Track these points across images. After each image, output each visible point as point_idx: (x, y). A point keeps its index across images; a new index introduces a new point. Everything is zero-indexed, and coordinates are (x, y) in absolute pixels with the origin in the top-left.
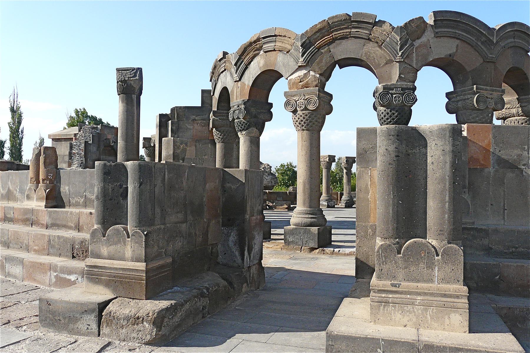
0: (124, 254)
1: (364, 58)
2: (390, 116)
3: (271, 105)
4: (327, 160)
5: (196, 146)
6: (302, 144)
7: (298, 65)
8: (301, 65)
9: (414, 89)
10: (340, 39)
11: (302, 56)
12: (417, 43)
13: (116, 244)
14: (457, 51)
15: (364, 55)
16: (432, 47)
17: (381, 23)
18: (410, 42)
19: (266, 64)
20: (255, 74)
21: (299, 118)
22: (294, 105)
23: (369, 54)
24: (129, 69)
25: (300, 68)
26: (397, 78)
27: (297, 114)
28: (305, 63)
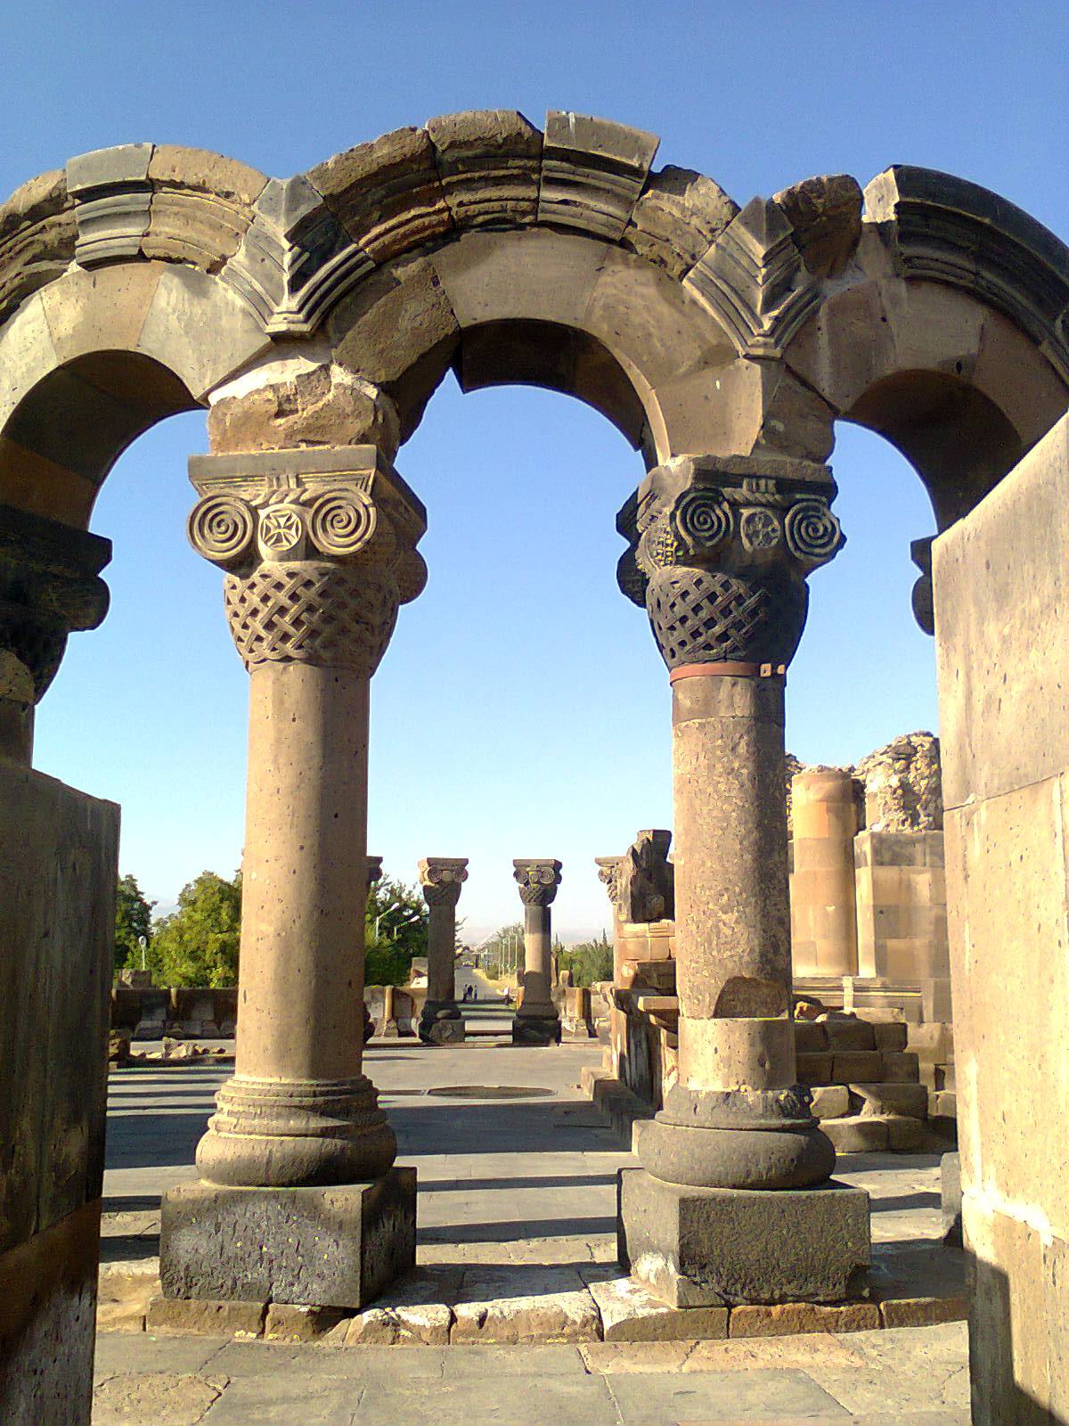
2: (726, 612)
3: (102, 550)
6: (279, 731)
7: (271, 329)
9: (830, 490)
10: (486, 227)
11: (295, 286)
12: (833, 290)
15: (598, 312)
16: (890, 316)
19: (90, 323)
20: (30, 370)
21: (265, 599)
22: (241, 526)
23: (627, 313)
25: (282, 345)
27: (255, 577)
28: (306, 321)
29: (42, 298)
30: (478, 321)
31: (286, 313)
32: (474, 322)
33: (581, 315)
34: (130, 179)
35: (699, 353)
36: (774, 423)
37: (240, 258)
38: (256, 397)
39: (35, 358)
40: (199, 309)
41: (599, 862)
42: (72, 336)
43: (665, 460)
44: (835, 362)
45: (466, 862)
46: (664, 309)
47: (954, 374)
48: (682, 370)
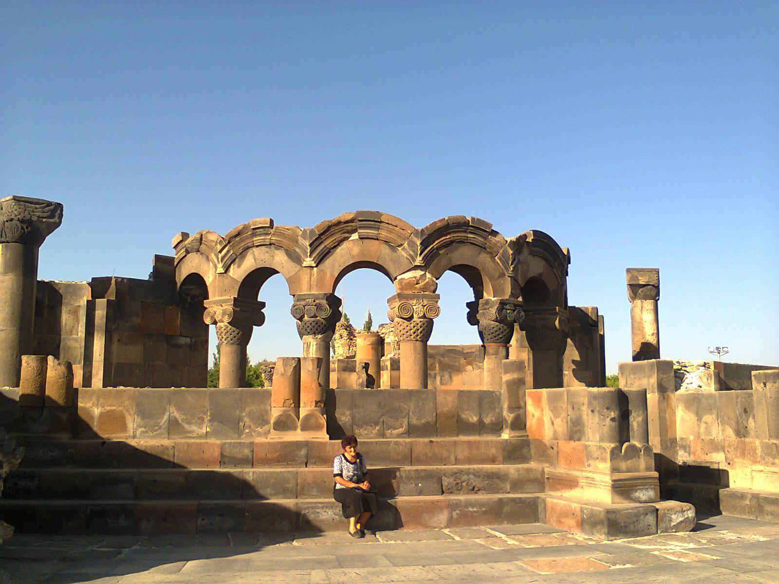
0: (639, 466)
2: (502, 333)
5: (144, 345)
6: (415, 357)
8: (419, 264)
10: (458, 242)
11: (421, 254)
13: (631, 458)
17: (495, 233)
19: (362, 252)
20: (344, 263)
21: (414, 327)
24: (41, 202)
25: (416, 268)
27: (412, 321)
28: (423, 263)
31: (419, 261)
37: (406, 245)
40: (394, 254)
42: (357, 256)
44: (521, 276)
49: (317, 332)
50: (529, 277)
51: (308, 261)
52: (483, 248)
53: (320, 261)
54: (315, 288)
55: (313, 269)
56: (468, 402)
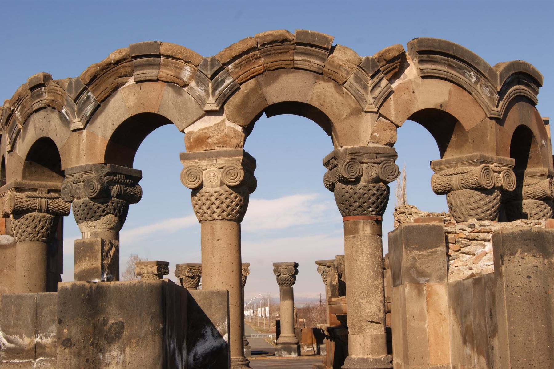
1: (316, 104)
4: (154, 269)
8: (210, 109)
9: (394, 156)
14: (449, 99)
15: (315, 98)
16: (416, 91)
18: (384, 82)
25: (210, 113)
26: (368, 138)
29: (121, 93)
30: (275, 103)
31: (211, 104)
32: (273, 103)
33: (309, 98)
34: (153, 53)
35: (349, 111)
36: (375, 134)
38: (201, 131)
39: (120, 114)
41: (318, 263)
43: (339, 147)
44: (395, 110)
45: (249, 265)
46: (337, 96)
47: (439, 108)
48: (344, 117)
49: (89, 216)
50: (416, 111)
51: (77, 123)
52: (319, 74)
53: (89, 120)
54: (84, 158)
55: (82, 133)
56: (18, 313)
